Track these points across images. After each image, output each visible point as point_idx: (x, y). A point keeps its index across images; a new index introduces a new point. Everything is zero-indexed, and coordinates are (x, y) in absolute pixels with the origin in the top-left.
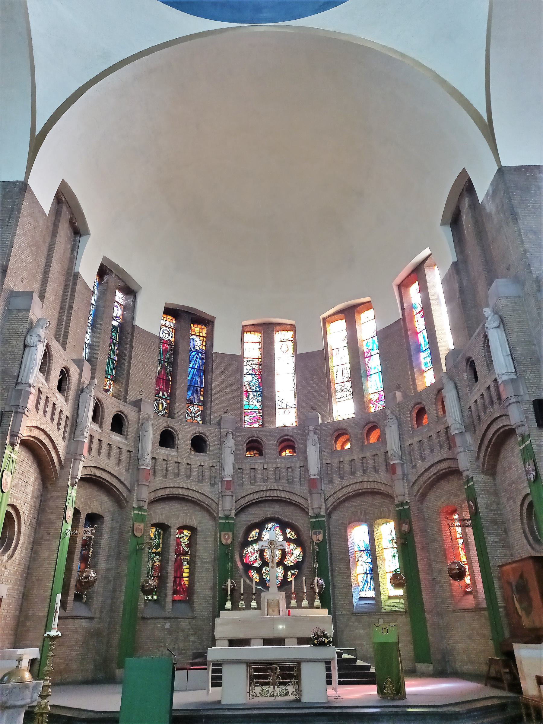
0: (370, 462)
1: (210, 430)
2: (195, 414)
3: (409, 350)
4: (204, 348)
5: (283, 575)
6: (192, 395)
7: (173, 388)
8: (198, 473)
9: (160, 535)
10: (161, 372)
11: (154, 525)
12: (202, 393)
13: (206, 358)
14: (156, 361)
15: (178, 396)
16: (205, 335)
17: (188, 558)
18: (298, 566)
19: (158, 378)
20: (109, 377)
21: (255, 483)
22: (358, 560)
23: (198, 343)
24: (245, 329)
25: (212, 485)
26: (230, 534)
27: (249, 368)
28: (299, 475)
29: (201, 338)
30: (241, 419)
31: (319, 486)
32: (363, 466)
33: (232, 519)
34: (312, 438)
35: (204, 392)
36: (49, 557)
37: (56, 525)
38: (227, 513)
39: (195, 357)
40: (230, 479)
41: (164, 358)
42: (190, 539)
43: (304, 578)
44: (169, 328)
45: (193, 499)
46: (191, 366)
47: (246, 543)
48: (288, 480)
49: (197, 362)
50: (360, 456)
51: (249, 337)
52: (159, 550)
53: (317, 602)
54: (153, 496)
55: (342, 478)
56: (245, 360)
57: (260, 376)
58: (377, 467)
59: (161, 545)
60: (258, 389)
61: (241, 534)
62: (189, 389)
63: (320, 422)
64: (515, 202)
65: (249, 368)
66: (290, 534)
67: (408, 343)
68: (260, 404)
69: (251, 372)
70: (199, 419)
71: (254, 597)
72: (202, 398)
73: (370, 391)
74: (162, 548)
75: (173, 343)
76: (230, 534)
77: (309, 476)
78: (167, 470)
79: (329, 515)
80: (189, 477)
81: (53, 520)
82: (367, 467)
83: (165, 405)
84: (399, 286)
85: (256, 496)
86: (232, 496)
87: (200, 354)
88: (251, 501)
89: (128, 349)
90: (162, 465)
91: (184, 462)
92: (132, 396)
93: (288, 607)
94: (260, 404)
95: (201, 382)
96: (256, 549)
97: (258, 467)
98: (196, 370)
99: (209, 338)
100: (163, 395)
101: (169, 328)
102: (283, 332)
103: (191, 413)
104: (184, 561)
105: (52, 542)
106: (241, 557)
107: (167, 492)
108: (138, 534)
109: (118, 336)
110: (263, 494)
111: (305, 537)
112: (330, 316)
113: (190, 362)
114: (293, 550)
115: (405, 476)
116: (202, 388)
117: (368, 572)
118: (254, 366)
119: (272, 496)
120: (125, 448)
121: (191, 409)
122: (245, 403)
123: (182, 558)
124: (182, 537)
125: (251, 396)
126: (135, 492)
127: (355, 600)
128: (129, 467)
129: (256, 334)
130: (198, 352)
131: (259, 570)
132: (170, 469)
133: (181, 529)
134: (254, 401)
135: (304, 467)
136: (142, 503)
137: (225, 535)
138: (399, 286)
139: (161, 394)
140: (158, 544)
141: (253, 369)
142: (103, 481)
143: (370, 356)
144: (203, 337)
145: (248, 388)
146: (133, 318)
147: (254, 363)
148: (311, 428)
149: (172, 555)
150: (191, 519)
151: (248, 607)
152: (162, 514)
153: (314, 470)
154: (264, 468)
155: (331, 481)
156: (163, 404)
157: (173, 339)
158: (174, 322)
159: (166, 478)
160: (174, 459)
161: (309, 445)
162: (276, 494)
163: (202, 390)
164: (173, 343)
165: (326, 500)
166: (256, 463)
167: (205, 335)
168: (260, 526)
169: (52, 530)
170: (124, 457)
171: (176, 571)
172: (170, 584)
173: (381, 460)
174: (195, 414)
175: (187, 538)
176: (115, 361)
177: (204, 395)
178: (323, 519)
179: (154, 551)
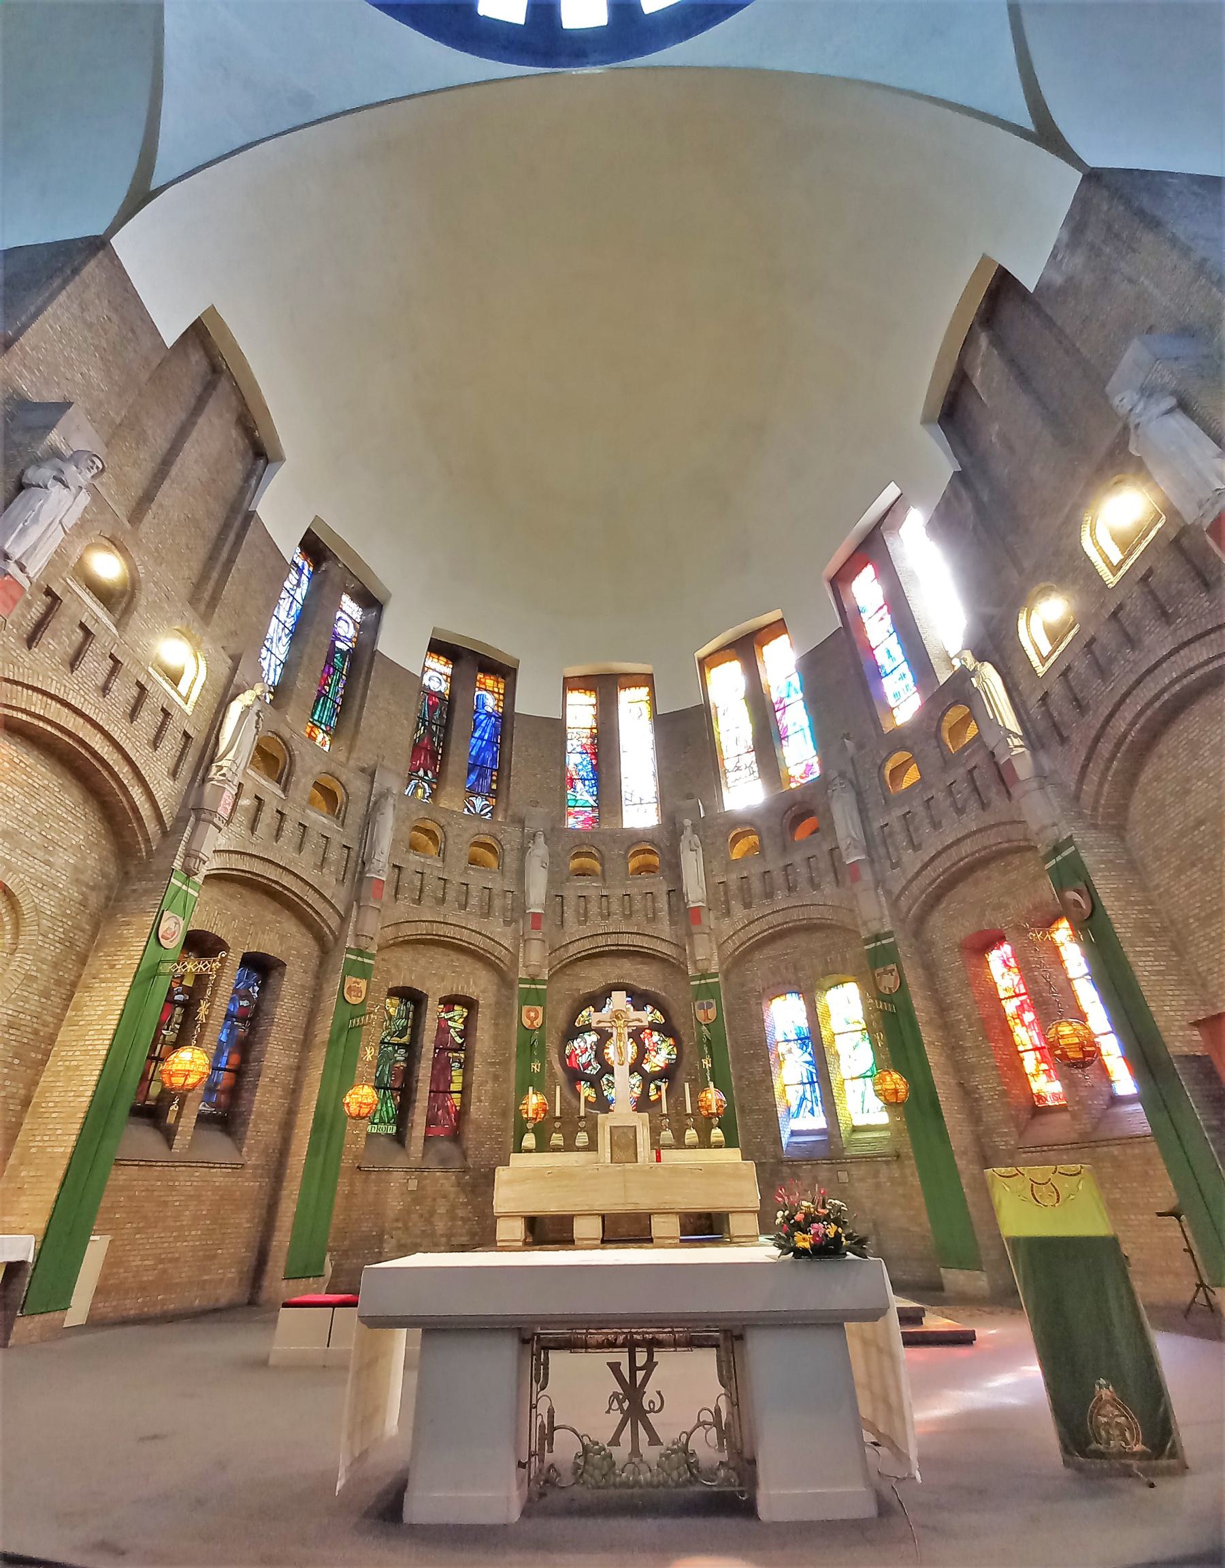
1: (504, 830)
2: (481, 811)
4: (500, 710)
5: (640, 1089)
6: (477, 779)
7: (443, 764)
8: (481, 899)
9: (408, 1011)
10: (423, 740)
11: (393, 992)
12: (494, 778)
13: (503, 725)
14: (413, 716)
15: (450, 777)
16: (502, 691)
17: (463, 1056)
18: (668, 1073)
19: (417, 748)
20: (323, 727)
21: (586, 921)
22: (784, 1058)
23: (490, 702)
24: (570, 684)
26: (540, 1009)
27: (575, 742)
28: (666, 907)
29: (496, 695)
30: (562, 819)
31: (704, 920)
32: (788, 880)
33: (543, 982)
35: (497, 777)
36: (103, 1017)
37: (131, 948)
38: (531, 970)
39: (485, 722)
40: (540, 911)
41: (431, 717)
42: (466, 1022)
43: (687, 1085)
44: (441, 674)
45: (471, 946)
46: (477, 735)
47: (573, 1032)
48: (646, 915)
49: (488, 730)
50: (781, 864)
51: (574, 697)
52: (405, 1039)
53: (717, 1134)
54: (390, 933)
55: (747, 905)
56: (569, 730)
57: (595, 754)
58: (816, 880)
59: (409, 1031)
60: (591, 775)
61: (562, 1015)
62: (470, 772)
65: (575, 742)
68: (595, 798)
69: (579, 749)
71: (582, 1124)
72: (494, 787)
73: (789, 762)
74: (411, 1035)
75: (447, 697)
76: (540, 1009)
77: (686, 904)
78: (421, 891)
81: (128, 938)
82: (796, 881)
83: (427, 791)
85: (587, 944)
86: (544, 941)
87: (493, 719)
88: (579, 953)
89: (360, 686)
90: (412, 882)
91: (456, 879)
93: (657, 1147)
94: (595, 798)
95: (494, 760)
96: (589, 1042)
97: (592, 894)
98: (484, 742)
99: (509, 696)
100: (426, 774)
101: (441, 674)
102: (633, 689)
103: (475, 808)
104: (453, 1062)
105: (116, 985)
106: (562, 1057)
107: (423, 929)
108: (353, 1000)
109: (345, 667)
110: (601, 941)
111: (678, 1022)
112: (710, 655)
113: (475, 730)
114: (659, 1042)
115: (879, 882)
116: (496, 770)
117: (806, 1081)
118: (584, 741)
119: (618, 945)
120: (337, 840)
121: (475, 801)
122: (569, 797)
123: (450, 1055)
124: (450, 1019)
125: (579, 785)
126: (353, 919)
127: (785, 1137)
128: (344, 875)
129: (588, 693)
130: (489, 715)
131: (594, 1082)
133: (449, 1002)
134: (585, 793)
135: (676, 892)
136: (364, 942)
137: (529, 1011)
139: (421, 773)
140: (405, 1028)
141: (582, 746)
142: (286, 892)
143: (784, 707)
144: (499, 693)
145: (574, 773)
147: (585, 735)
148: (687, 822)
150: (468, 984)
151: (569, 1147)
152: (411, 971)
154: (602, 896)
156: (425, 789)
157: (448, 692)
158: (451, 666)
159: (419, 904)
160: (436, 873)
161: (684, 852)
162: (625, 940)
163: (495, 773)
164: (447, 697)
165: (720, 947)
167: (502, 691)
168: (597, 1000)
169: (121, 957)
170: (334, 855)
171: (433, 1079)
173: (824, 864)
174: (481, 811)
175: (461, 1020)
176: (338, 704)
178: (716, 980)
179: (396, 1040)
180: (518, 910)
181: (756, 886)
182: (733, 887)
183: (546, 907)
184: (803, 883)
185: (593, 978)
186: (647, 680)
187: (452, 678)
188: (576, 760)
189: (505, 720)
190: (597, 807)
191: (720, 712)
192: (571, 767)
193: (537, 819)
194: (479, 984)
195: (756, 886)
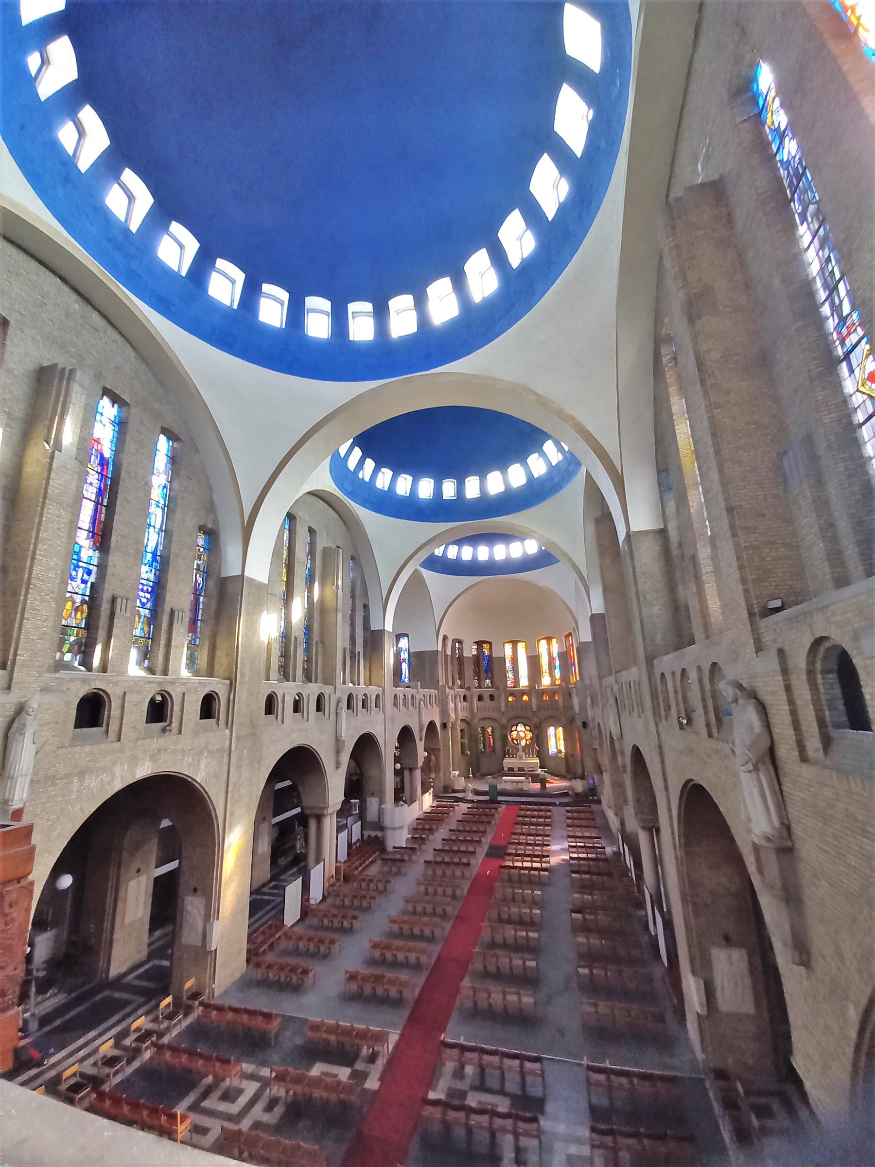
7: (480, 675)
18: (531, 739)
25: (498, 712)
34: (534, 694)
63: (537, 688)
66: (528, 728)
70: (490, 685)
79: (541, 723)
84: (565, 636)
99: (491, 650)
125: (509, 673)
135: (531, 705)
149: (486, 736)
151: (513, 757)
172: (487, 746)
180: (499, 710)
185: (515, 722)
187: (477, 649)
188: (508, 665)
189: (490, 656)
190: (515, 679)
193: (501, 687)
194: (494, 724)
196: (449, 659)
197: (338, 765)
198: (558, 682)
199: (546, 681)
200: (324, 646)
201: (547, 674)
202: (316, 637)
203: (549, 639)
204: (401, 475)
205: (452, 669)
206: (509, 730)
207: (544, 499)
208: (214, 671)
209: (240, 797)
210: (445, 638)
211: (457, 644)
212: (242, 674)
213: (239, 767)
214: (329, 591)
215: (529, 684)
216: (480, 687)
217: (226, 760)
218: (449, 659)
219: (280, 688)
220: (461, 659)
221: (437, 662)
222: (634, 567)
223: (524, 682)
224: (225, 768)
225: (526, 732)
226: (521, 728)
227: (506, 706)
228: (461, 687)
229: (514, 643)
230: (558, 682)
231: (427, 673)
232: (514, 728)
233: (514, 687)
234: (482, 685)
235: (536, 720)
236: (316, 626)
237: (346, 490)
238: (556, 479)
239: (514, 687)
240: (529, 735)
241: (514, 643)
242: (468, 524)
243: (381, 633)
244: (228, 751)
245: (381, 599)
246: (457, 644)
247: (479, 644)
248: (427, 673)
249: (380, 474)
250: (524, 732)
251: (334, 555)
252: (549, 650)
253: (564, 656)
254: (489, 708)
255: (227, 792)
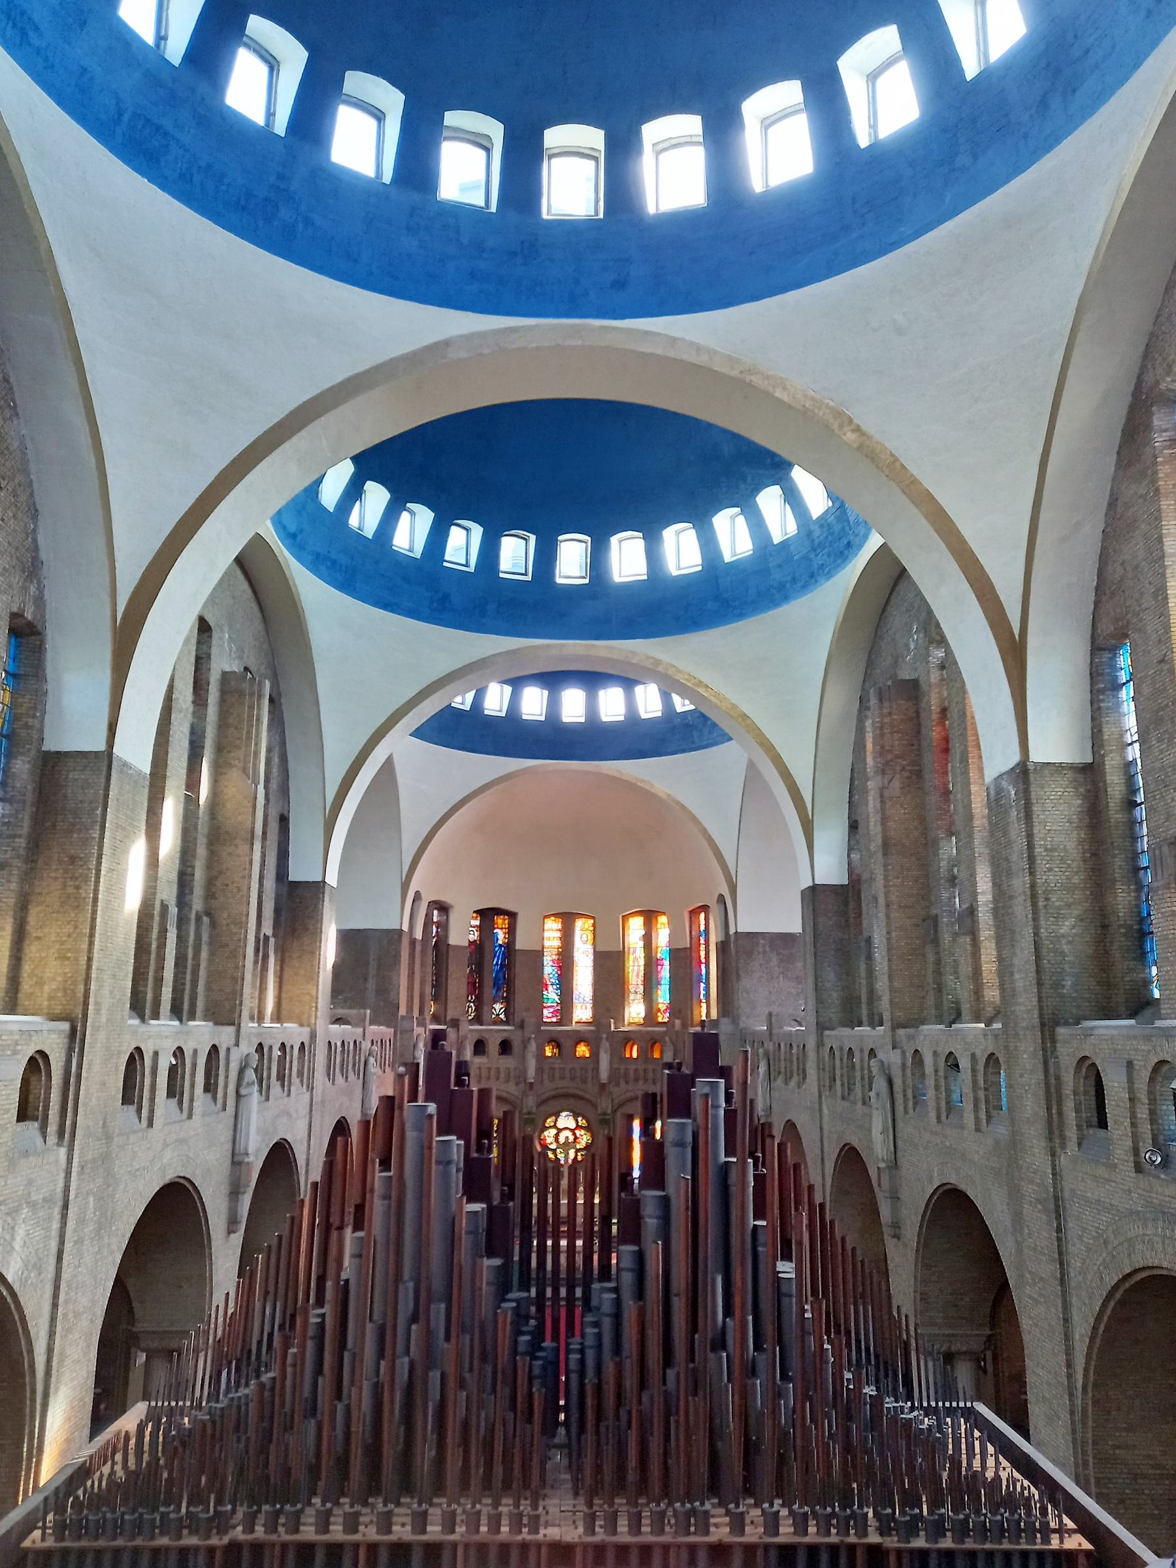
0: (651, 1074)
3: (691, 980)
13: (508, 952)
23: (501, 936)
25: (517, 1084)
34: (605, 1045)
55: (627, 1083)
57: (560, 967)
63: (612, 1029)
64: (741, 965)
67: (691, 974)
70: (502, 1016)
80: (498, 1079)
84: (691, 912)
85: (554, 1093)
92: (451, 1014)
99: (511, 931)
125: (550, 988)
130: (501, 946)
131: (554, 1151)
132: (483, 1075)
135: (596, 1069)
138: (691, 912)
141: (553, 961)
146: (447, 937)
153: (604, 1075)
155: (618, 1085)
162: (571, 1091)
165: (612, 1100)
166: (553, 1063)
168: (557, 1115)
177: (506, 991)
180: (521, 1077)
181: (632, 1075)
182: (622, 1071)
183: (535, 1078)
184: (650, 1081)
185: (555, 1104)
186: (593, 918)
187: (480, 928)
188: (549, 970)
189: (509, 946)
191: (631, 950)
192: (546, 977)
193: (531, 1021)
195: (632, 1075)
196: (418, 948)
197: (232, 1223)
198: (663, 1018)
199: (635, 1011)
200: (213, 924)
201: (640, 996)
202: (197, 904)
203: (650, 917)
204: (408, 505)
205: (424, 973)
206: (540, 1126)
207: (741, 616)
208: (20, 995)
209: (77, 1315)
210: (417, 896)
211: (436, 912)
212: (98, 1011)
213: (79, 1242)
214: (234, 783)
215: (594, 1016)
216: (478, 1019)
217: (56, 1225)
218: (418, 948)
219: (149, 1037)
220: (441, 950)
221: (397, 956)
222: (1030, 837)
223: (583, 1012)
224: (54, 1245)
225: (577, 1132)
226: (566, 1121)
227: (540, 1070)
228: (436, 1019)
229: (568, 919)
230: (663, 1018)
231: (371, 984)
232: (550, 1122)
233: (558, 1023)
234: (485, 1017)
235: (605, 1105)
236: (199, 875)
237: (284, 527)
238: (777, 576)
239: (558, 1023)
240: (584, 1139)
241: (568, 919)
242: (548, 646)
243: (318, 887)
244: (60, 1203)
245: (322, 804)
246: (436, 912)
247: (487, 915)
248: (371, 984)
249: (405, 516)
250: (573, 1131)
251: (252, 694)
252: (648, 939)
253: (684, 959)
254: (498, 1070)
255: (55, 1305)
